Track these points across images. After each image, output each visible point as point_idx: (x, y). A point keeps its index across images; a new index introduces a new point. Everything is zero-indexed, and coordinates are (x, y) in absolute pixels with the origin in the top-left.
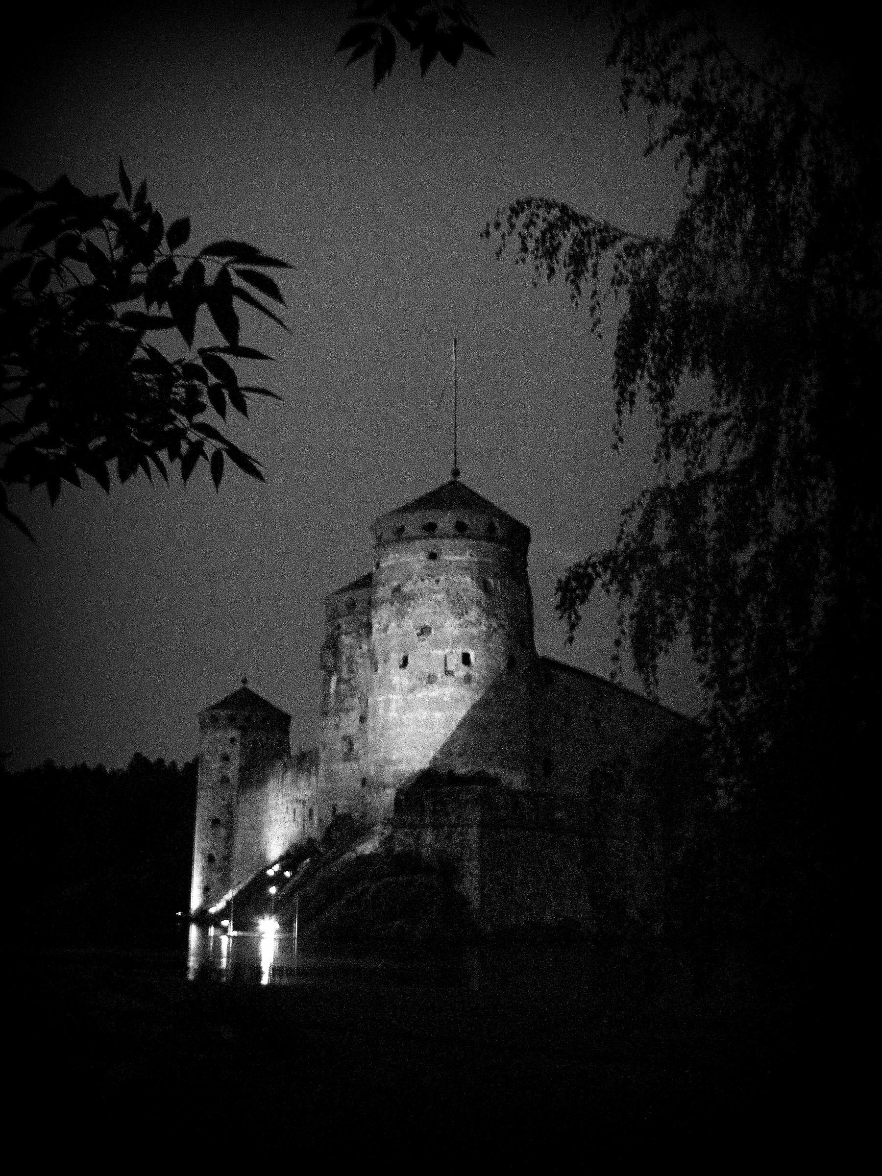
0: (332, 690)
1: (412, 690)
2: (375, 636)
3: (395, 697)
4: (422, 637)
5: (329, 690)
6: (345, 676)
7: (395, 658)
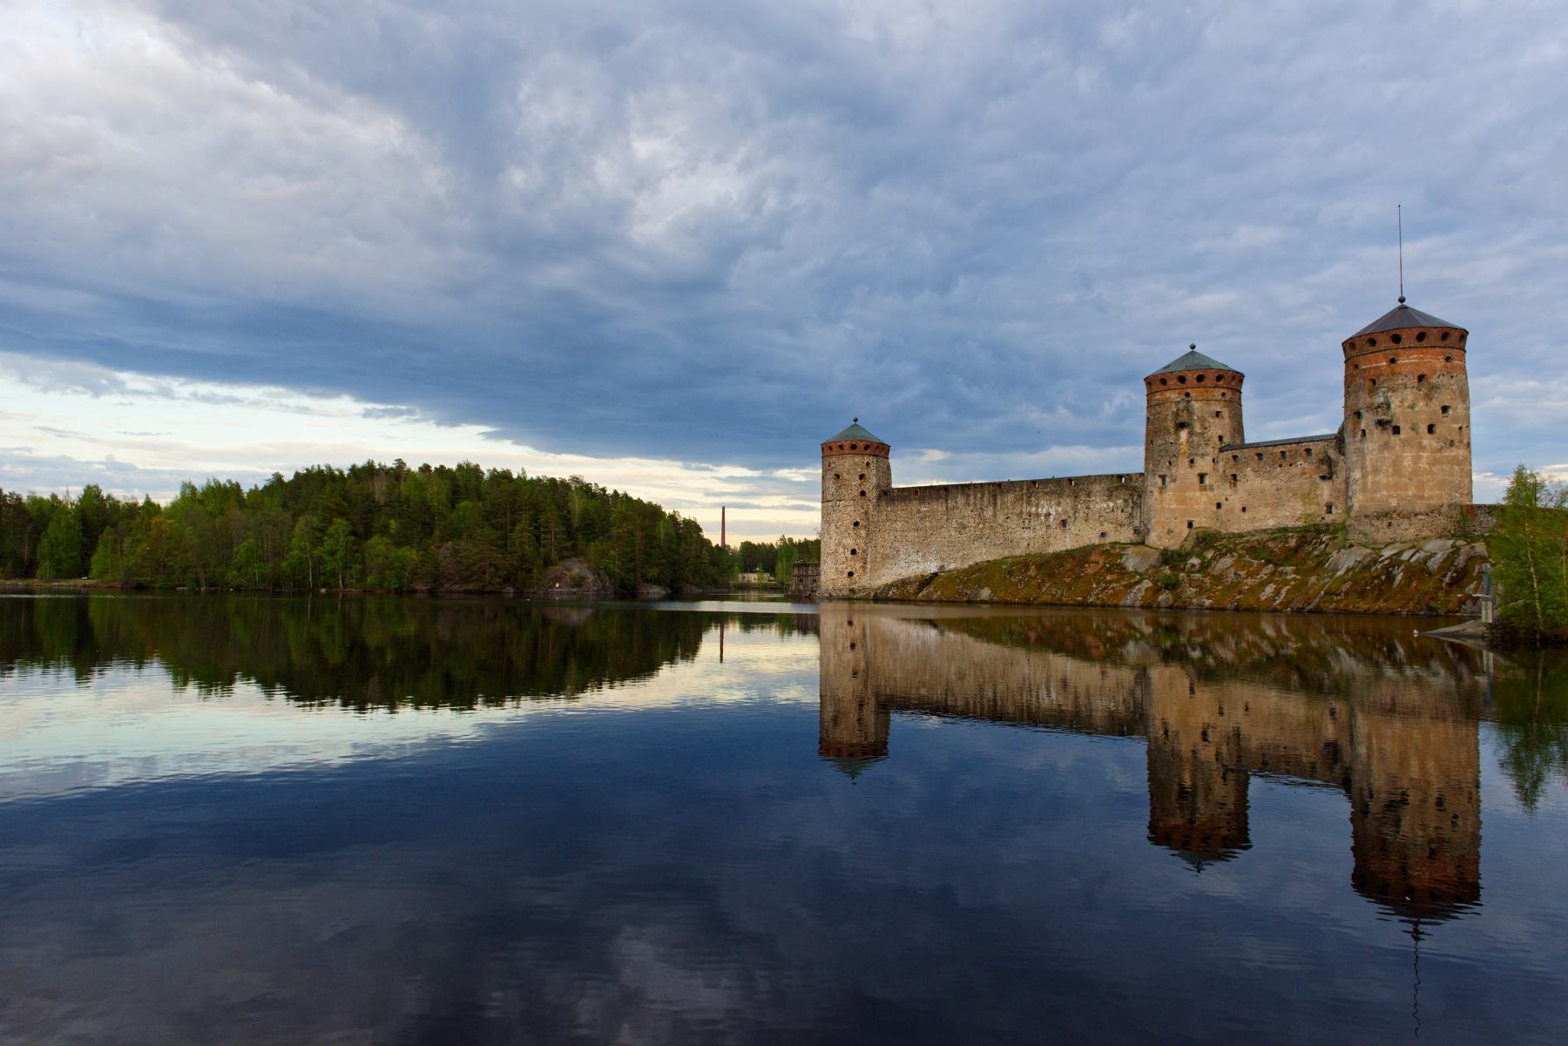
6: (1197, 429)
7: (1423, 428)
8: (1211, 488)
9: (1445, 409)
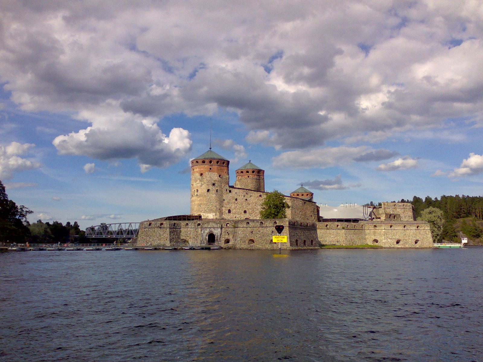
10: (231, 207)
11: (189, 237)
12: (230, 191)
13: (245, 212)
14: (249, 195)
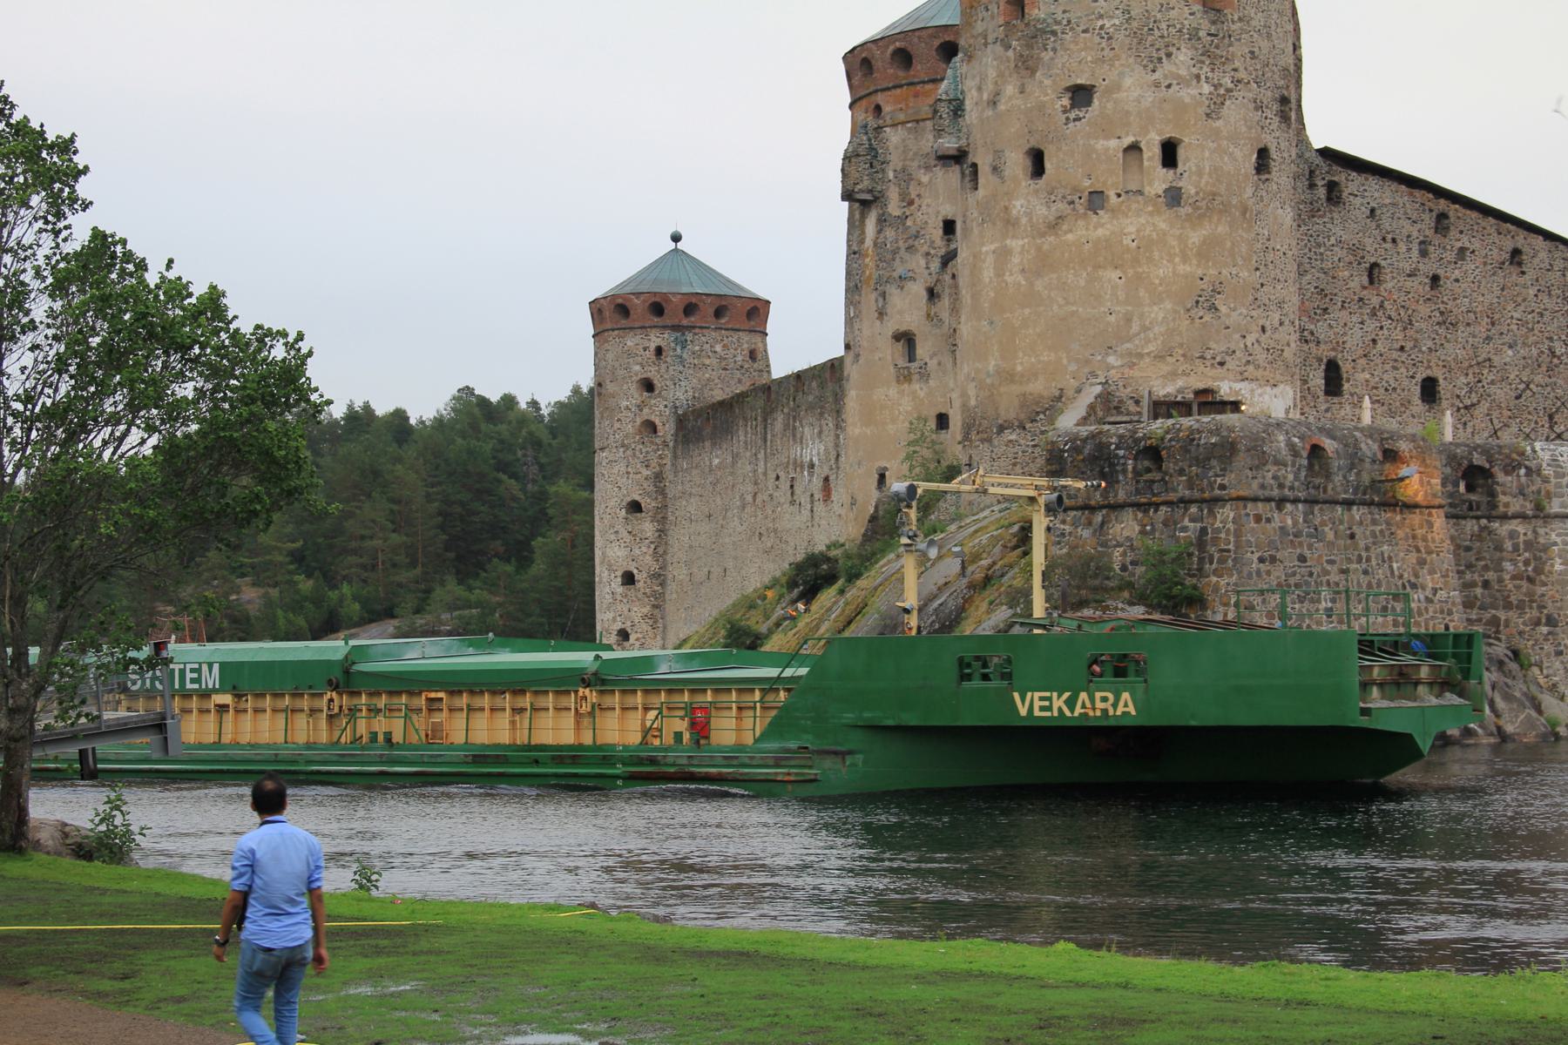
0: (869, 242)
1: (1054, 226)
2: (972, 114)
3: (1015, 244)
4: (1072, 115)
5: (862, 242)
6: (894, 208)
7: (1016, 163)
8: (924, 375)
9: (1081, 95)
10: (1339, 346)
11: (1521, 606)
12: (1333, 193)
13: (1429, 390)
14: (1456, 240)
